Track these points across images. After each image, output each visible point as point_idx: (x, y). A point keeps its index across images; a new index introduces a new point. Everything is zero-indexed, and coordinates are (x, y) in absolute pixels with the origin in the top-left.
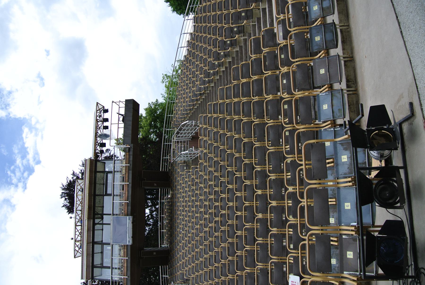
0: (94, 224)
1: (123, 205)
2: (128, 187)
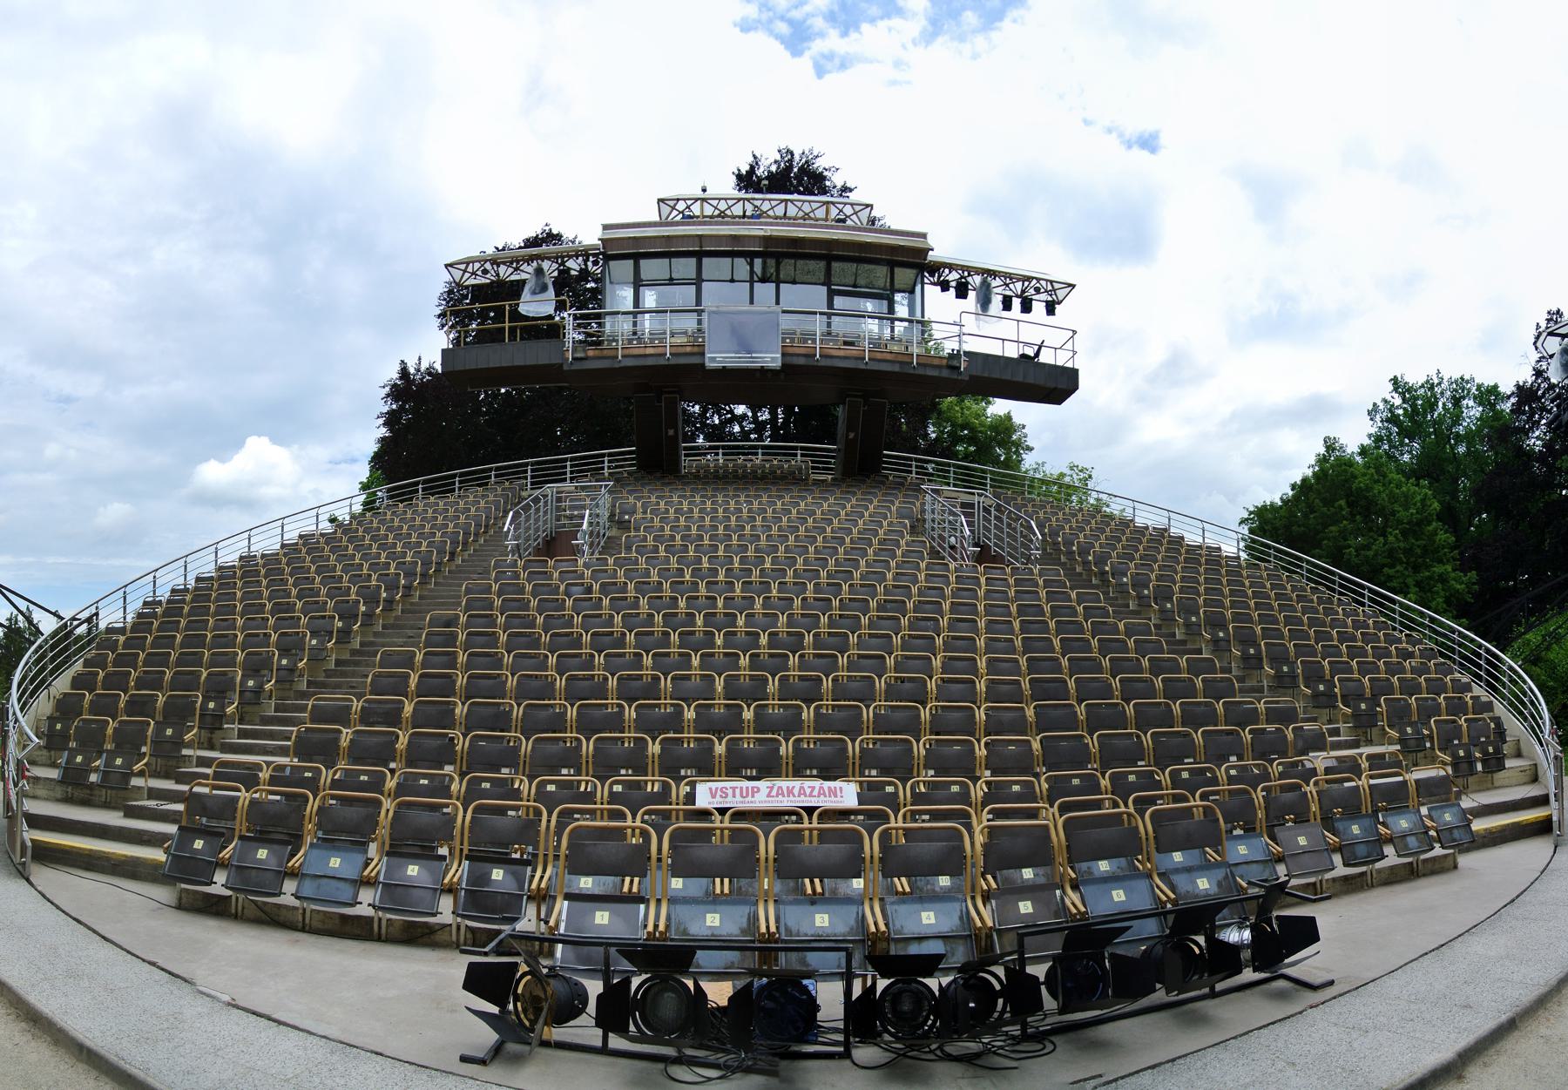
1: (805, 341)
2: (857, 358)
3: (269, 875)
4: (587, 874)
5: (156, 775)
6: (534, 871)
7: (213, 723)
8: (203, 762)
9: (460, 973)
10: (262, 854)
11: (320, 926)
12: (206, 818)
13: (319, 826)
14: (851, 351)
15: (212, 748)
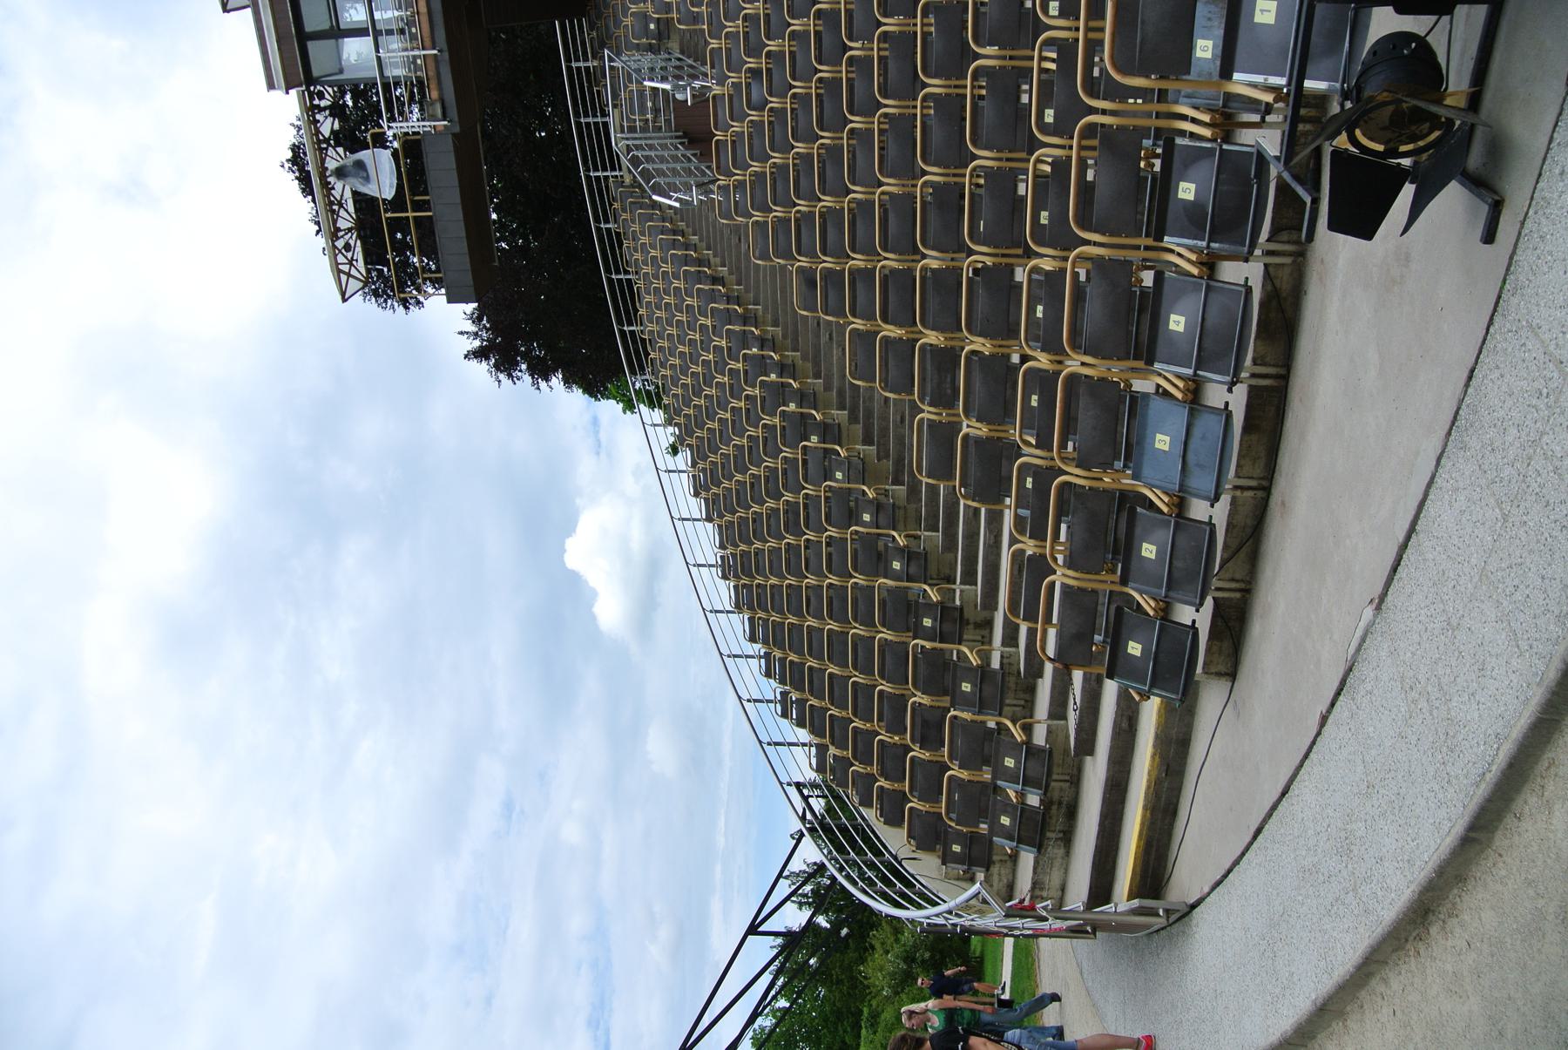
3: (1182, 541)
4: (1190, 48)
5: (1029, 706)
6: (1182, 133)
7: (954, 622)
8: (1011, 638)
9: (1346, 245)
10: (1148, 551)
11: (1262, 463)
12: (1095, 634)
13: (1106, 465)
15: (988, 624)
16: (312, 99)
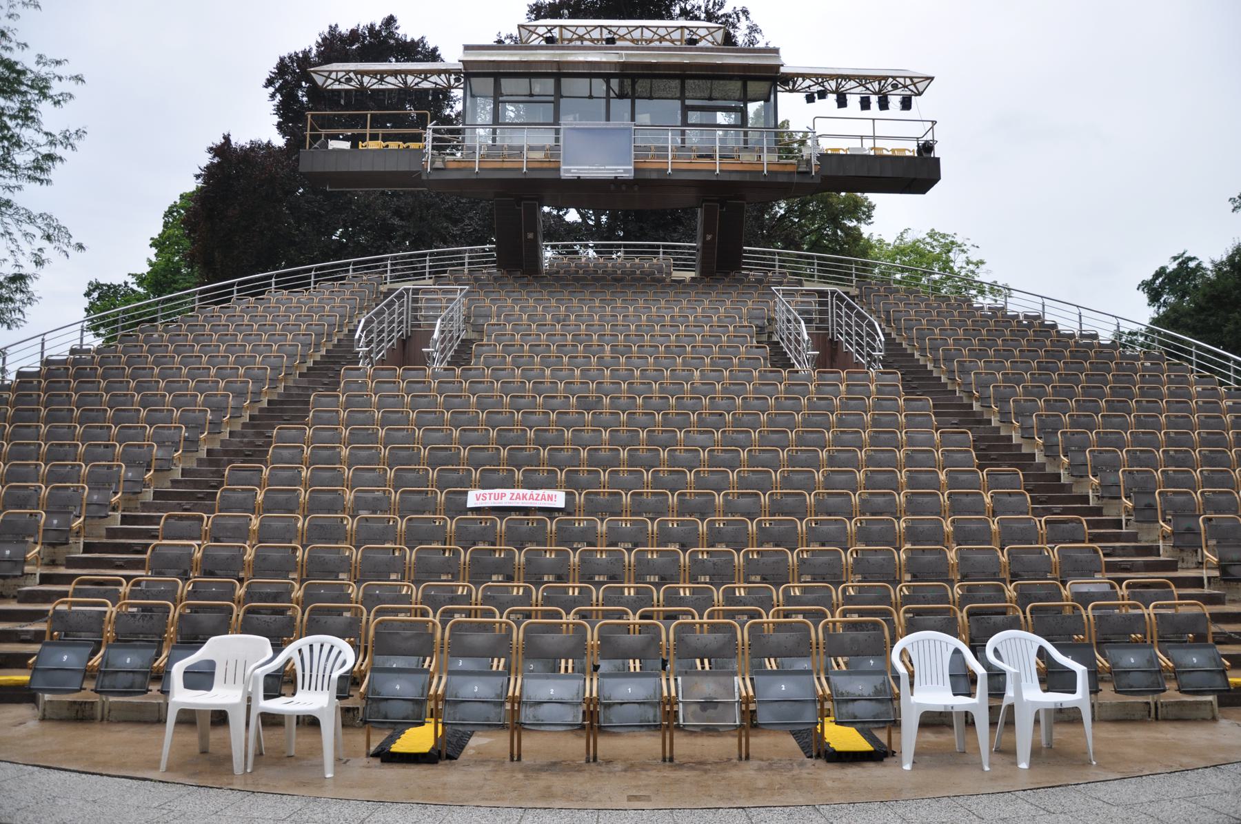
0: (607, 77)
14: (704, 164)
16: (456, 74)
